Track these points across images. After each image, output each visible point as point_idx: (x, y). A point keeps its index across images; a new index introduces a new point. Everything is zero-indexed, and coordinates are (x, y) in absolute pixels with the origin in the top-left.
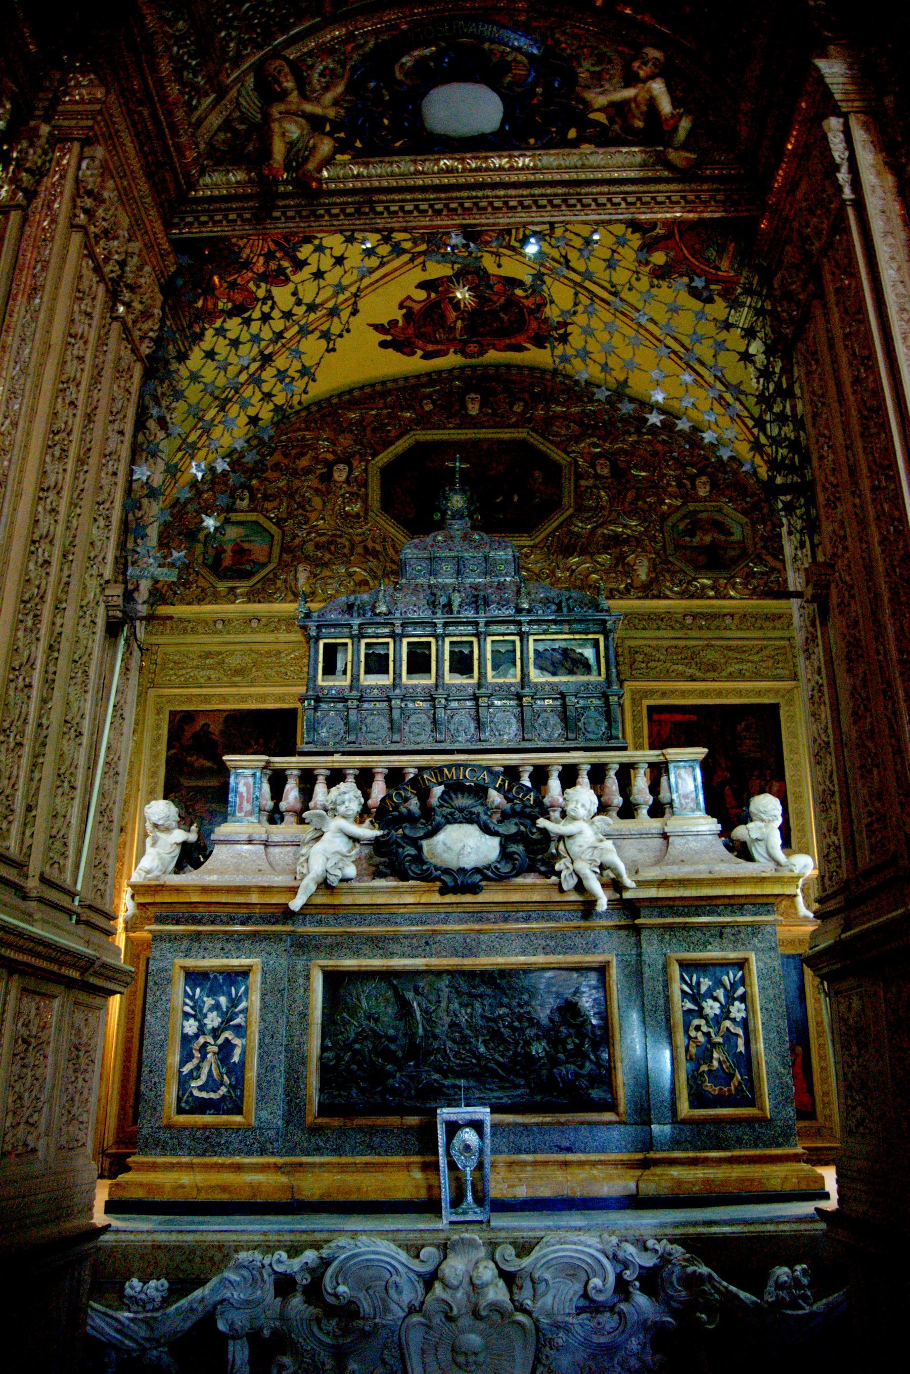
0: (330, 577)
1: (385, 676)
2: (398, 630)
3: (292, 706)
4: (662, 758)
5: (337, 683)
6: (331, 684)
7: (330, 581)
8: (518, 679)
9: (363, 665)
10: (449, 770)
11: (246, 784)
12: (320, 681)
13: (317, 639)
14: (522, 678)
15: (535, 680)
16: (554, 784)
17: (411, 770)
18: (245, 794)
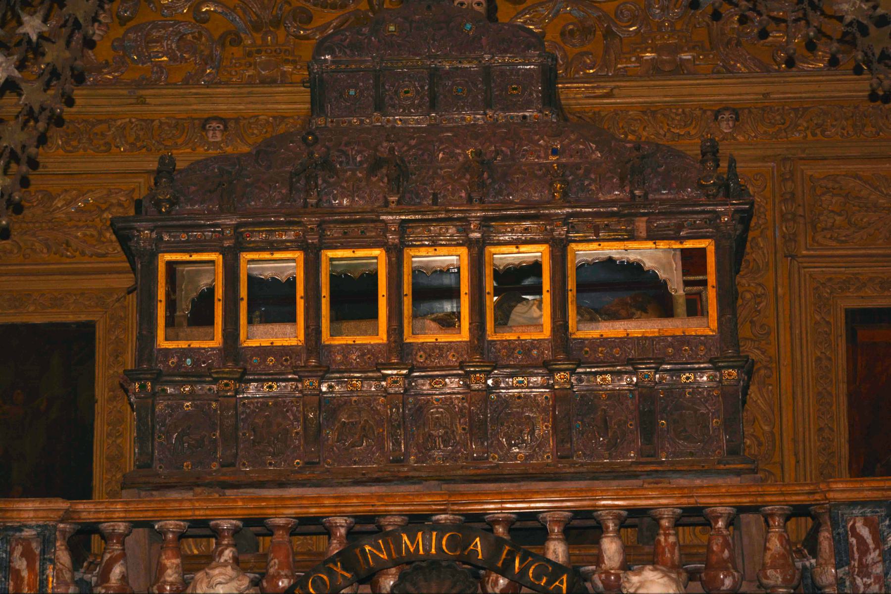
0: (155, 26)
1: (288, 328)
2: (312, 240)
3: (83, 318)
4: (817, 497)
5: (195, 344)
6: (183, 344)
7: (155, 34)
8: (546, 333)
9: (243, 306)
10: (413, 539)
11: (27, 554)
12: (162, 343)
13: (153, 256)
14: (554, 330)
15: (580, 335)
16: (611, 548)
17: (340, 521)
18: (25, 574)
